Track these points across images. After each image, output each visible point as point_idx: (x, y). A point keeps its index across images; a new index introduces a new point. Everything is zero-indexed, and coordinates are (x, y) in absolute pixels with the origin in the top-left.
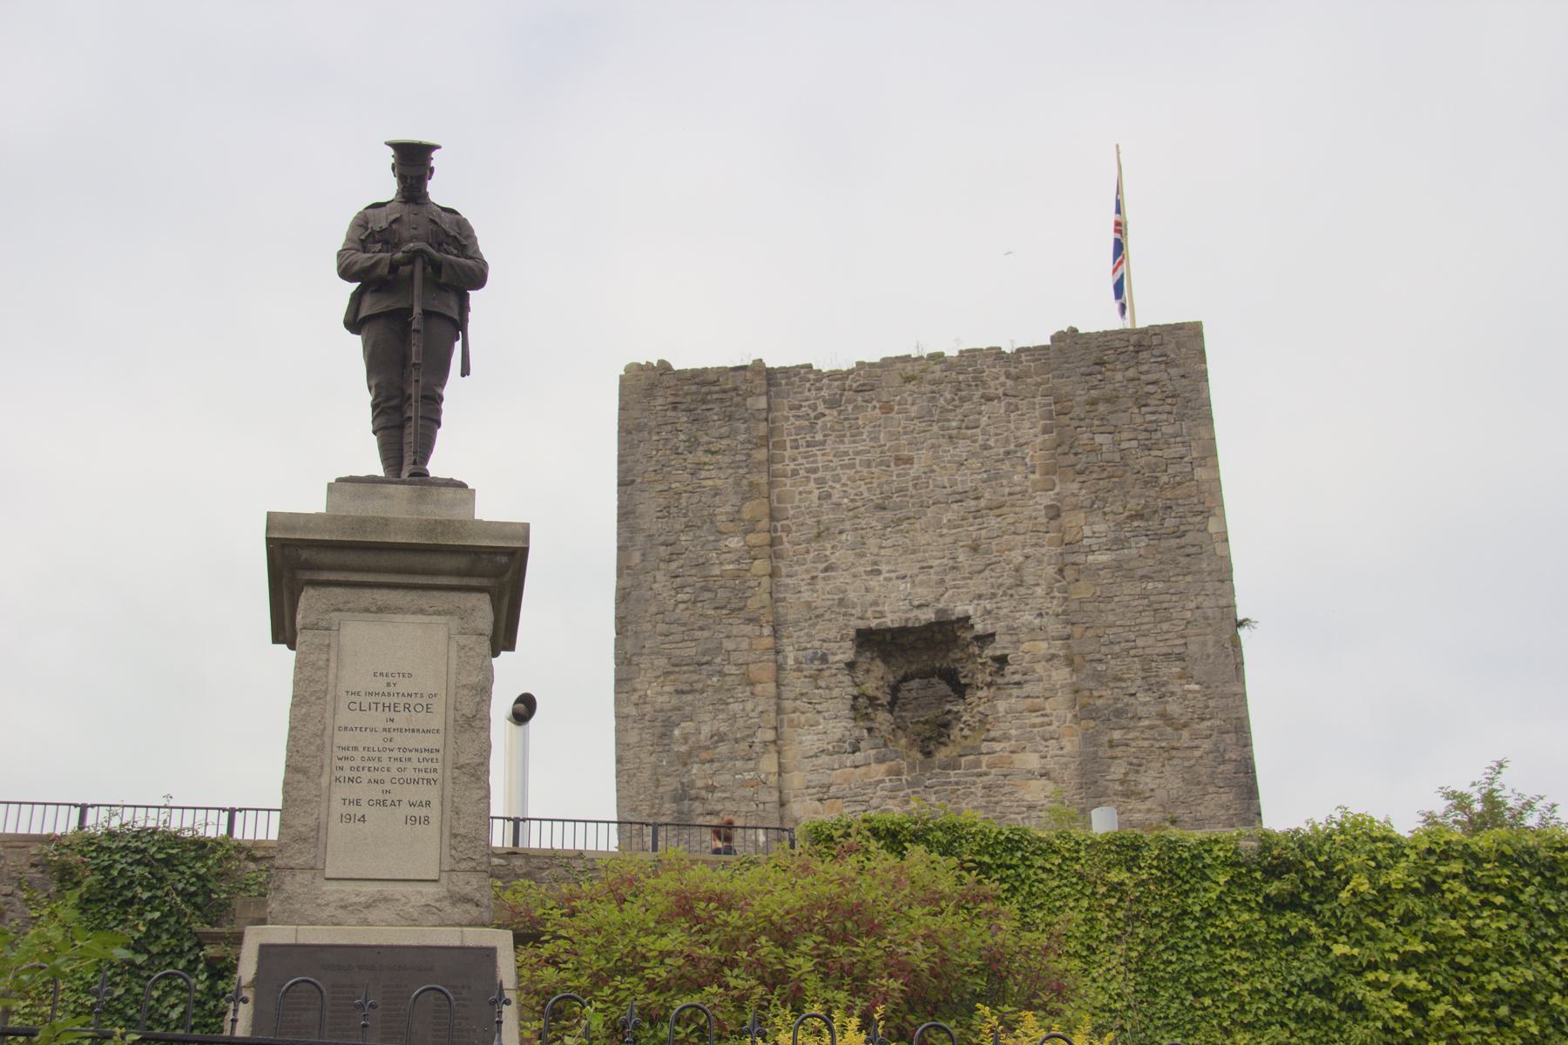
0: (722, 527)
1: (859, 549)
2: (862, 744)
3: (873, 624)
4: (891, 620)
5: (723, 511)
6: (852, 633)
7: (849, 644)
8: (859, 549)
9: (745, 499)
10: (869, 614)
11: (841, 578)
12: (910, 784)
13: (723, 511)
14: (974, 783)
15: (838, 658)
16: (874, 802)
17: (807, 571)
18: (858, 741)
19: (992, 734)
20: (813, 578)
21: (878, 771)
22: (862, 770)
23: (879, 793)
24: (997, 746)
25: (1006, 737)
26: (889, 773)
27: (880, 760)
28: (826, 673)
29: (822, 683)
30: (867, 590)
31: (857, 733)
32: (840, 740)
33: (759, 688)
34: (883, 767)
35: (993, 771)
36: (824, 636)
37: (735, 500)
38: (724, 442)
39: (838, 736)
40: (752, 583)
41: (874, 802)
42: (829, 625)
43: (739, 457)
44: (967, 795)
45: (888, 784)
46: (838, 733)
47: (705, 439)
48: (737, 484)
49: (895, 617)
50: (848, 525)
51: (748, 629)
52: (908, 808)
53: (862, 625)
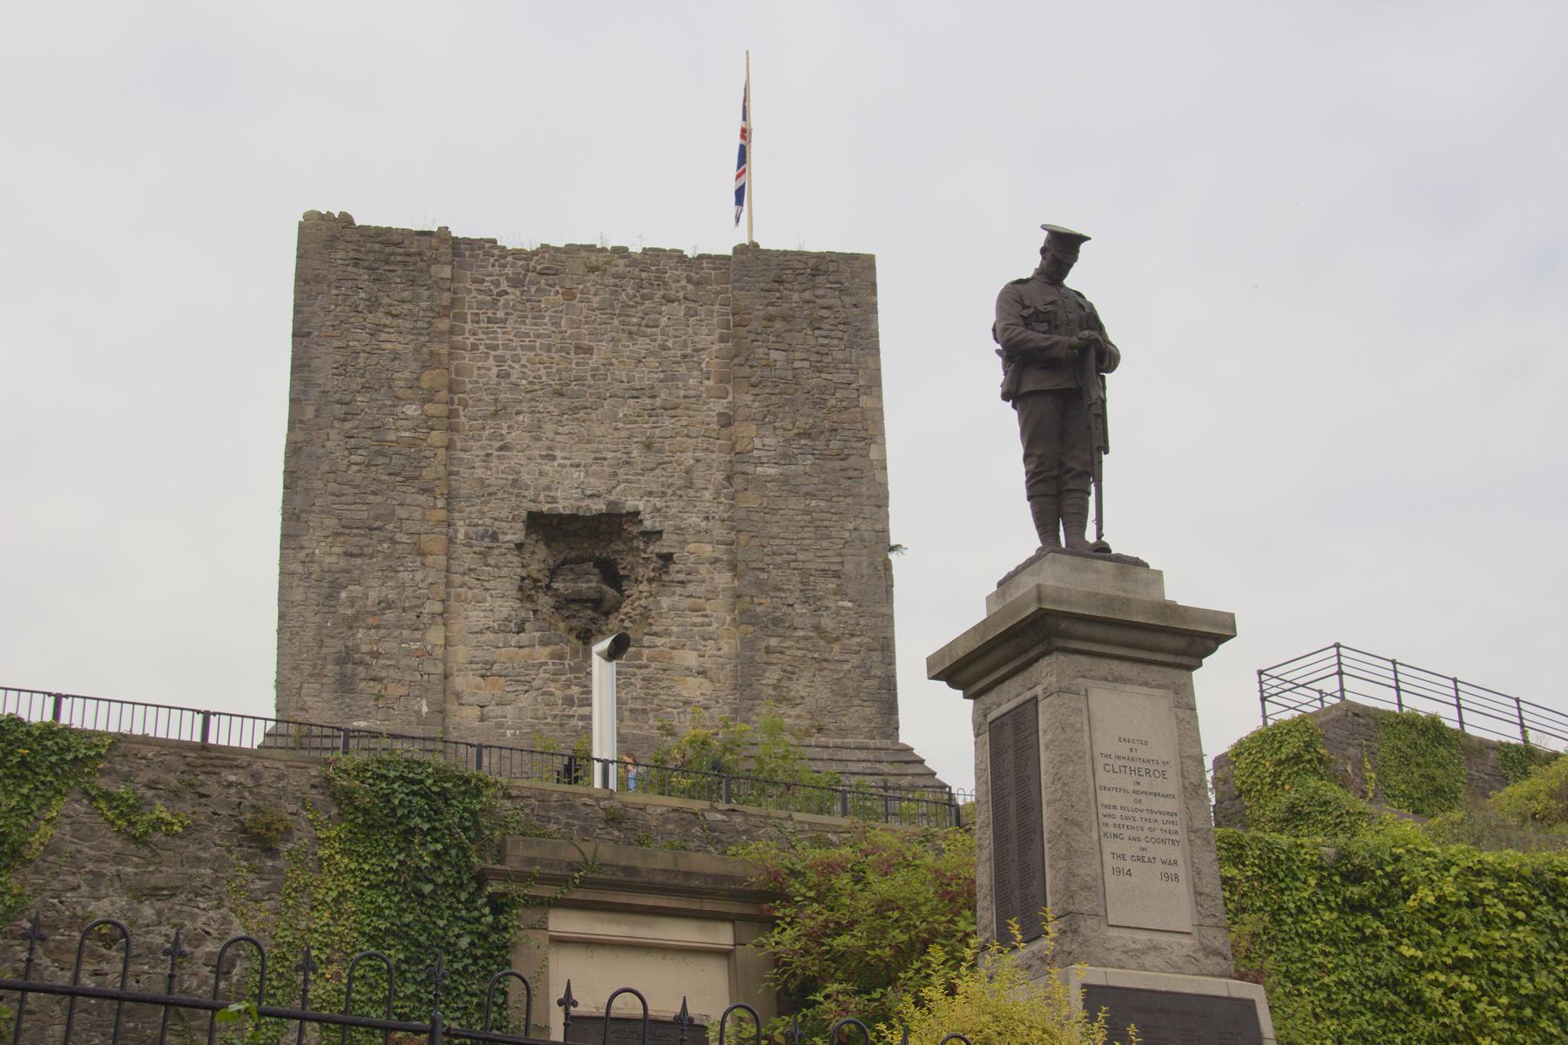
1: (535, 431)
3: (545, 508)
4: (563, 506)
6: (524, 515)
7: (520, 525)
8: (535, 431)
10: (542, 498)
11: (516, 458)
14: (634, 675)
15: (508, 537)
16: (537, 683)
17: (482, 448)
18: (523, 621)
19: (655, 629)
21: (542, 653)
22: (527, 650)
24: (659, 641)
25: (667, 633)
26: (553, 656)
27: (544, 643)
28: (496, 552)
29: (491, 561)
30: (541, 474)
32: (506, 619)
34: (547, 650)
36: (496, 515)
39: (504, 615)
40: (428, 454)
41: (537, 683)
45: (551, 667)
46: (505, 612)
49: (566, 503)
50: (525, 407)
51: (422, 499)
52: (568, 692)
53: (534, 507)
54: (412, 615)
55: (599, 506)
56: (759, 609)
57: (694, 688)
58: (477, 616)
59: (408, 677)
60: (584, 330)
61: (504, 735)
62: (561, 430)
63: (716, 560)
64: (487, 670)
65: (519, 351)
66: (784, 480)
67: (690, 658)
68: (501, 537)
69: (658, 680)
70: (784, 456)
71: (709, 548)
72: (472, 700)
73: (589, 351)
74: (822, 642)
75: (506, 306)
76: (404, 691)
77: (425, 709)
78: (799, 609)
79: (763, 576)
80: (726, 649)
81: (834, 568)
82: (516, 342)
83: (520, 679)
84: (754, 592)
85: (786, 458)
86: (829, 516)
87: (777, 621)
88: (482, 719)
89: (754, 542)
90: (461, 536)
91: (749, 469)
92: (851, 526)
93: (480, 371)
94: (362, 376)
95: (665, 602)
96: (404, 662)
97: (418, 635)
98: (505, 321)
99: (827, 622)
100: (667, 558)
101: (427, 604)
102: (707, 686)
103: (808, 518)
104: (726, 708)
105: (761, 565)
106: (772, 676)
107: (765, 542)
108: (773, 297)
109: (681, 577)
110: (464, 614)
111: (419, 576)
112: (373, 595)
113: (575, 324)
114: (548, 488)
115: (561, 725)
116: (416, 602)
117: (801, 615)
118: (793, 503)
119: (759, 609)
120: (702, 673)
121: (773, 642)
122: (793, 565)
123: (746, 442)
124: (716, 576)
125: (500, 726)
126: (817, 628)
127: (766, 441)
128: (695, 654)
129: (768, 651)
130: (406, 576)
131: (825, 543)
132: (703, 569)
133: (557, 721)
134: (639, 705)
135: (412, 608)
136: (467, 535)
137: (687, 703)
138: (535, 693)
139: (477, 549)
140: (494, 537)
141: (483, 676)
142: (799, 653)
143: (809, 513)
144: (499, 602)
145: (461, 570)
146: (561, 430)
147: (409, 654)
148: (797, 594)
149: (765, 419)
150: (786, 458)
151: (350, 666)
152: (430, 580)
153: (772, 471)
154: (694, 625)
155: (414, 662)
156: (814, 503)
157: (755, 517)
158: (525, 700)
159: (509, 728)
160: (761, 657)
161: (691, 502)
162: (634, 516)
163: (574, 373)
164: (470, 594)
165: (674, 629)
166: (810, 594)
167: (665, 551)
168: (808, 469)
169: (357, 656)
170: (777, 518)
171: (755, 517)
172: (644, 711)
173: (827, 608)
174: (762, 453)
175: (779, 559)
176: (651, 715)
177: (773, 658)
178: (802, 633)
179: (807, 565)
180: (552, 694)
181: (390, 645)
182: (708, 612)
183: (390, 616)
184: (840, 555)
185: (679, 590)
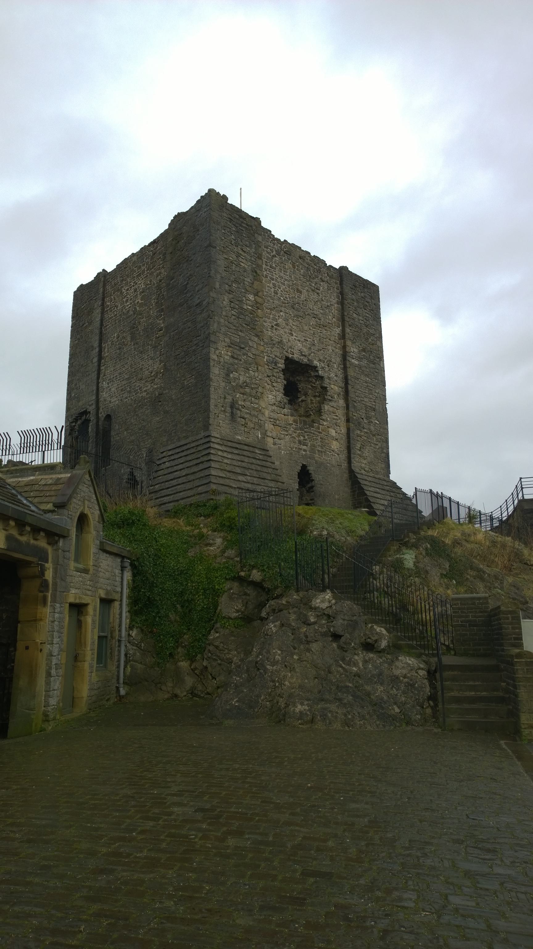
3: (291, 356)
22: (287, 417)
27: (292, 416)
51: (256, 339)
62: (294, 323)
114: (291, 347)
116: (256, 386)
125: (279, 448)
146: (294, 323)
147: (254, 408)
152: (260, 377)
154: (334, 419)
162: (315, 368)
183: (248, 390)
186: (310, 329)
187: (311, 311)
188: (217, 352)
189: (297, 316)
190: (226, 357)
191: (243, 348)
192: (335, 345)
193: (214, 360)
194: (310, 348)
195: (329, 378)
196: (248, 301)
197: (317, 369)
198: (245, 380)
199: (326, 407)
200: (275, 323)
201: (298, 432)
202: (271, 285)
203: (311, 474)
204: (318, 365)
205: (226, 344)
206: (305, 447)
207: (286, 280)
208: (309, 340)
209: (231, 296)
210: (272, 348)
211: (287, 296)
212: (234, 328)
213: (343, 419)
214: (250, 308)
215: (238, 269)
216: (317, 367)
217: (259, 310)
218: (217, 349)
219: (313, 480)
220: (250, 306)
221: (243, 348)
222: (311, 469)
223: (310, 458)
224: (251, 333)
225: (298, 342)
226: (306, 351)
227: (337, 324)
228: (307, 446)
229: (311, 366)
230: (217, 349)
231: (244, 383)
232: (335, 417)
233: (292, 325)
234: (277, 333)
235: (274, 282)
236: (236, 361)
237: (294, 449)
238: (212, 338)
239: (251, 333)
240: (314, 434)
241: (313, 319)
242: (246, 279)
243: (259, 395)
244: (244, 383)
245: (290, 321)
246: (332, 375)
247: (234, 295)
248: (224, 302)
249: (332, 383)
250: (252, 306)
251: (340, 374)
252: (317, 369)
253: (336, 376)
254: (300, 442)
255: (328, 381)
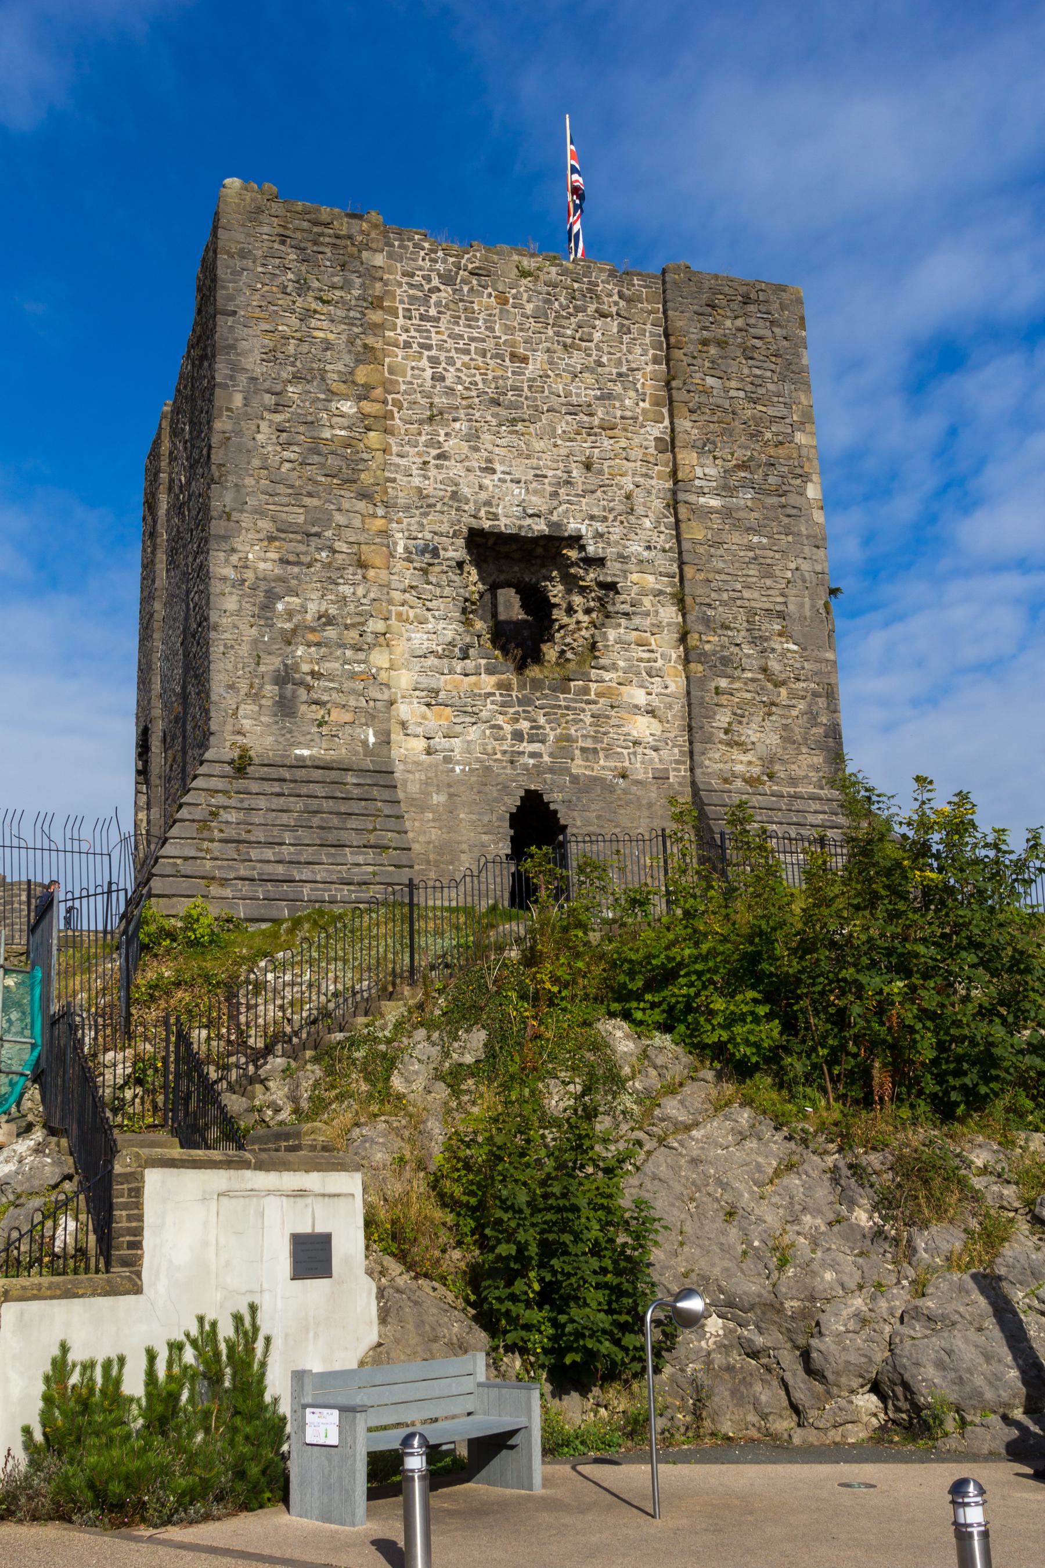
0: (335, 386)
1: (473, 437)
2: (471, 651)
3: (486, 525)
4: (506, 523)
5: (335, 368)
6: (465, 530)
8: (473, 437)
9: (358, 362)
10: (482, 514)
11: (454, 469)
12: (520, 702)
13: (335, 368)
14: (584, 711)
15: (450, 554)
16: (484, 714)
17: (419, 454)
18: (469, 646)
19: (602, 661)
20: (425, 463)
21: (488, 682)
22: (473, 679)
23: (489, 706)
24: (607, 676)
25: (614, 667)
26: (500, 686)
27: (490, 671)
28: (437, 569)
30: (481, 487)
31: (468, 640)
32: (450, 643)
33: (371, 573)
34: (493, 680)
35: (601, 700)
36: (436, 529)
37: (348, 359)
38: (338, 293)
40: (365, 456)
41: (484, 714)
42: (440, 517)
43: (352, 314)
44: (576, 721)
45: (498, 698)
46: (449, 635)
47: (316, 284)
48: (351, 342)
51: (361, 505)
52: (517, 726)
53: (475, 523)
54: (353, 635)
55: (540, 527)
56: (707, 647)
57: (643, 727)
58: (419, 639)
59: (352, 703)
60: (519, 337)
61: (453, 770)
62: (499, 442)
63: (660, 593)
64: (432, 698)
65: (453, 354)
66: (727, 513)
67: (639, 696)
68: (442, 553)
69: (608, 717)
70: (726, 487)
71: (651, 579)
72: (420, 730)
73: (525, 360)
74: (770, 686)
75: (438, 304)
76: (348, 717)
77: (372, 739)
78: (747, 650)
79: (710, 612)
80: (672, 688)
81: (778, 608)
82: (450, 344)
83: (467, 709)
84: (701, 628)
85: (726, 489)
86: (772, 554)
87: (725, 661)
88: (429, 752)
89: (701, 576)
90: (400, 549)
91: (692, 498)
92: (793, 566)
93: (410, 368)
94: (293, 365)
95: (612, 634)
96: (348, 685)
97: (361, 656)
98: (437, 320)
99: (774, 665)
100: (611, 587)
101: (371, 622)
102: (656, 727)
103: (751, 554)
104: (676, 750)
105: (708, 600)
106: (723, 718)
107: (711, 576)
108: (707, 321)
109: (626, 608)
110: (406, 635)
111: (360, 591)
112: (313, 607)
113: (508, 329)
114: (488, 503)
115: (512, 762)
116: (358, 619)
117: (748, 656)
118: (736, 538)
119: (707, 647)
120: (651, 712)
121: (723, 683)
122: (739, 603)
123: (688, 469)
124: (661, 610)
125: (447, 760)
126: (764, 670)
127: (707, 471)
128: (643, 691)
129: (718, 691)
130: (346, 590)
131: (769, 582)
132: (647, 602)
133: (507, 757)
134: (589, 744)
135: (353, 625)
136: (406, 549)
137: (636, 743)
138: (484, 726)
139: (417, 565)
140: (435, 552)
141: (428, 705)
142: (748, 696)
143: (751, 548)
144: (442, 624)
145: (402, 587)
146: (499, 442)
147: (353, 676)
148: (743, 633)
149: (704, 447)
150: (726, 489)
151: (289, 686)
152: (372, 595)
153: (715, 503)
154: (641, 660)
155: (359, 686)
156: (756, 539)
157: (701, 549)
158: (473, 733)
159: (458, 763)
160: (710, 697)
161: (633, 529)
162: (575, 541)
163: (510, 382)
164: (411, 613)
165: (621, 663)
166: (757, 634)
167: (609, 579)
168: (749, 504)
169: (297, 676)
170: (721, 552)
171: (701, 549)
172: (595, 751)
173: (773, 650)
174: (703, 483)
175: (725, 596)
176: (601, 754)
177: (723, 699)
178: (750, 675)
179: (753, 604)
180: (500, 728)
181: (333, 666)
182: (654, 647)
183: (331, 633)
184: (783, 595)
185: (623, 621)
186: (556, 446)
187: (563, 400)
188: (234, 559)
189: (513, 422)
190: (262, 565)
191: (318, 535)
192: (644, 470)
193: (224, 579)
194: (555, 494)
195: (623, 558)
196: (335, 420)
197: (582, 542)
198: (323, 609)
199: (612, 634)
200: (434, 452)
201: (512, 710)
202: (424, 363)
203: (556, 812)
204: (584, 532)
205: (261, 536)
206: (536, 747)
207: (472, 339)
208: (550, 473)
209: (278, 418)
210: (425, 514)
211: (478, 378)
212: (290, 491)
213: (675, 653)
214: (343, 433)
215: (305, 348)
216: (580, 537)
217: (372, 434)
218: (234, 550)
219: (566, 827)
220: (341, 428)
221: (318, 535)
222: (555, 798)
223: (551, 770)
224: (342, 493)
225: (514, 486)
226: (539, 504)
227: (651, 416)
228: (543, 742)
229: (562, 539)
230: (234, 550)
231: (319, 618)
232: (646, 655)
233: (490, 447)
234: (440, 477)
235: (433, 353)
236: (296, 570)
237: (499, 756)
238: (217, 527)
239: (342, 493)
240: (567, 708)
241: (569, 418)
242: (328, 367)
243: (369, 640)
244: (319, 618)
245: (486, 437)
246: (635, 548)
247: (292, 413)
248: (259, 437)
249: (633, 568)
250: (349, 428)
251: (664, 540)
252: (582, 542)
253: (649, 548)
254: (518, 736)
255: (618, 565)
